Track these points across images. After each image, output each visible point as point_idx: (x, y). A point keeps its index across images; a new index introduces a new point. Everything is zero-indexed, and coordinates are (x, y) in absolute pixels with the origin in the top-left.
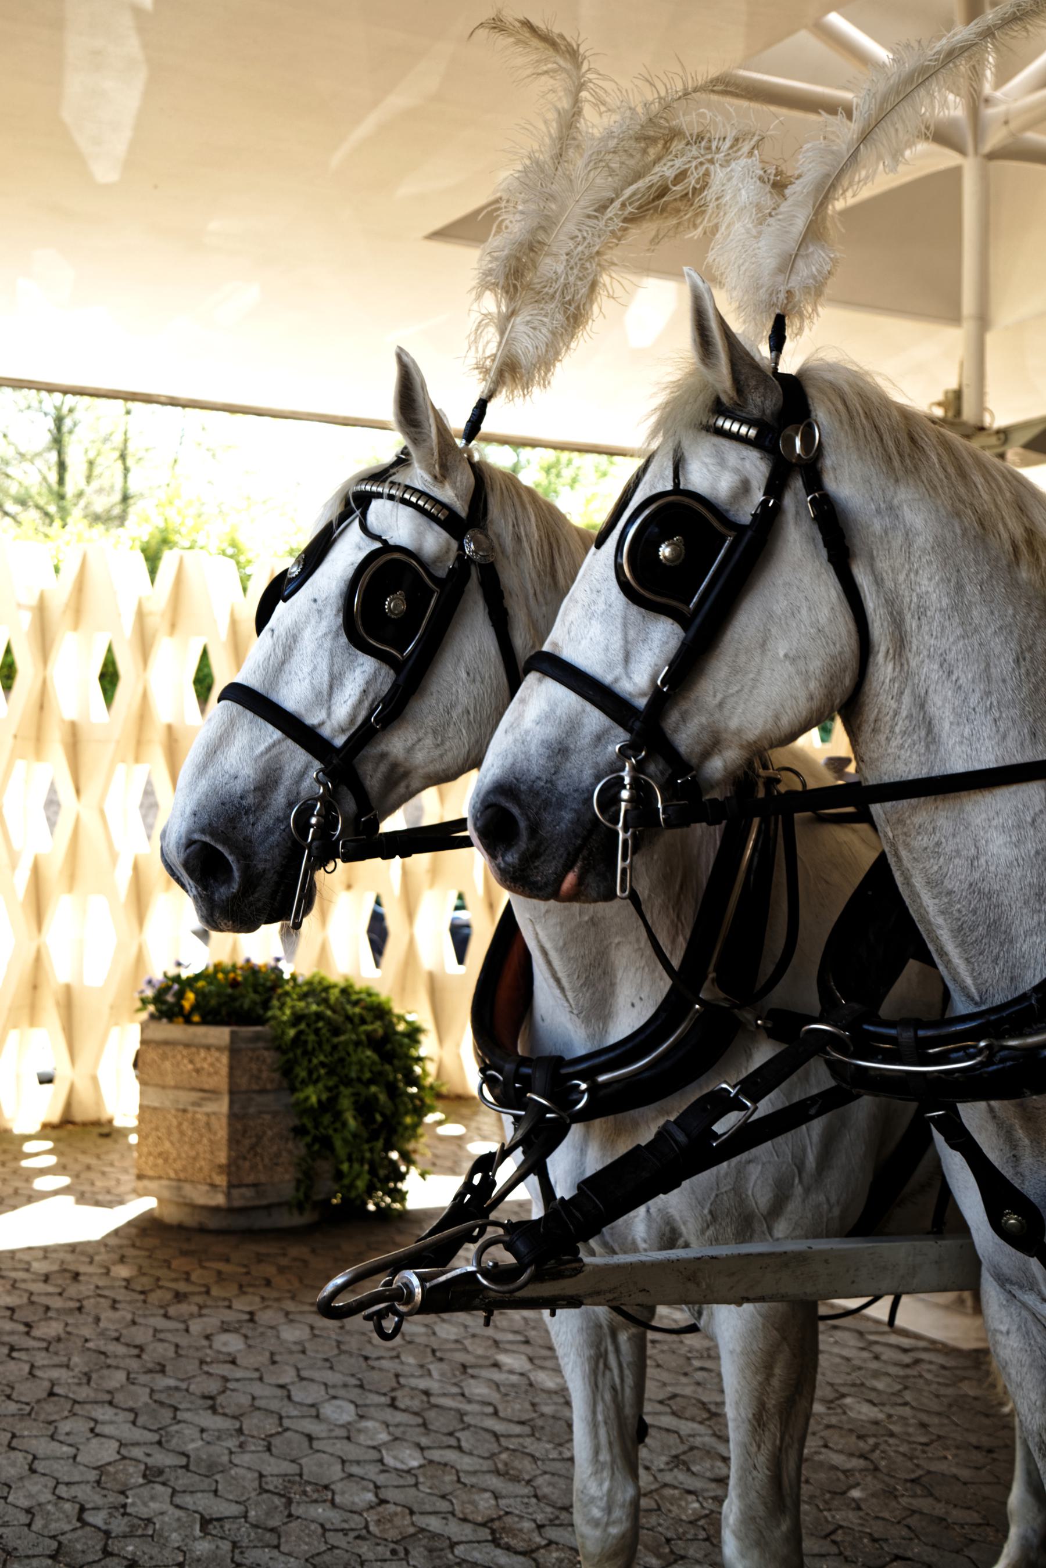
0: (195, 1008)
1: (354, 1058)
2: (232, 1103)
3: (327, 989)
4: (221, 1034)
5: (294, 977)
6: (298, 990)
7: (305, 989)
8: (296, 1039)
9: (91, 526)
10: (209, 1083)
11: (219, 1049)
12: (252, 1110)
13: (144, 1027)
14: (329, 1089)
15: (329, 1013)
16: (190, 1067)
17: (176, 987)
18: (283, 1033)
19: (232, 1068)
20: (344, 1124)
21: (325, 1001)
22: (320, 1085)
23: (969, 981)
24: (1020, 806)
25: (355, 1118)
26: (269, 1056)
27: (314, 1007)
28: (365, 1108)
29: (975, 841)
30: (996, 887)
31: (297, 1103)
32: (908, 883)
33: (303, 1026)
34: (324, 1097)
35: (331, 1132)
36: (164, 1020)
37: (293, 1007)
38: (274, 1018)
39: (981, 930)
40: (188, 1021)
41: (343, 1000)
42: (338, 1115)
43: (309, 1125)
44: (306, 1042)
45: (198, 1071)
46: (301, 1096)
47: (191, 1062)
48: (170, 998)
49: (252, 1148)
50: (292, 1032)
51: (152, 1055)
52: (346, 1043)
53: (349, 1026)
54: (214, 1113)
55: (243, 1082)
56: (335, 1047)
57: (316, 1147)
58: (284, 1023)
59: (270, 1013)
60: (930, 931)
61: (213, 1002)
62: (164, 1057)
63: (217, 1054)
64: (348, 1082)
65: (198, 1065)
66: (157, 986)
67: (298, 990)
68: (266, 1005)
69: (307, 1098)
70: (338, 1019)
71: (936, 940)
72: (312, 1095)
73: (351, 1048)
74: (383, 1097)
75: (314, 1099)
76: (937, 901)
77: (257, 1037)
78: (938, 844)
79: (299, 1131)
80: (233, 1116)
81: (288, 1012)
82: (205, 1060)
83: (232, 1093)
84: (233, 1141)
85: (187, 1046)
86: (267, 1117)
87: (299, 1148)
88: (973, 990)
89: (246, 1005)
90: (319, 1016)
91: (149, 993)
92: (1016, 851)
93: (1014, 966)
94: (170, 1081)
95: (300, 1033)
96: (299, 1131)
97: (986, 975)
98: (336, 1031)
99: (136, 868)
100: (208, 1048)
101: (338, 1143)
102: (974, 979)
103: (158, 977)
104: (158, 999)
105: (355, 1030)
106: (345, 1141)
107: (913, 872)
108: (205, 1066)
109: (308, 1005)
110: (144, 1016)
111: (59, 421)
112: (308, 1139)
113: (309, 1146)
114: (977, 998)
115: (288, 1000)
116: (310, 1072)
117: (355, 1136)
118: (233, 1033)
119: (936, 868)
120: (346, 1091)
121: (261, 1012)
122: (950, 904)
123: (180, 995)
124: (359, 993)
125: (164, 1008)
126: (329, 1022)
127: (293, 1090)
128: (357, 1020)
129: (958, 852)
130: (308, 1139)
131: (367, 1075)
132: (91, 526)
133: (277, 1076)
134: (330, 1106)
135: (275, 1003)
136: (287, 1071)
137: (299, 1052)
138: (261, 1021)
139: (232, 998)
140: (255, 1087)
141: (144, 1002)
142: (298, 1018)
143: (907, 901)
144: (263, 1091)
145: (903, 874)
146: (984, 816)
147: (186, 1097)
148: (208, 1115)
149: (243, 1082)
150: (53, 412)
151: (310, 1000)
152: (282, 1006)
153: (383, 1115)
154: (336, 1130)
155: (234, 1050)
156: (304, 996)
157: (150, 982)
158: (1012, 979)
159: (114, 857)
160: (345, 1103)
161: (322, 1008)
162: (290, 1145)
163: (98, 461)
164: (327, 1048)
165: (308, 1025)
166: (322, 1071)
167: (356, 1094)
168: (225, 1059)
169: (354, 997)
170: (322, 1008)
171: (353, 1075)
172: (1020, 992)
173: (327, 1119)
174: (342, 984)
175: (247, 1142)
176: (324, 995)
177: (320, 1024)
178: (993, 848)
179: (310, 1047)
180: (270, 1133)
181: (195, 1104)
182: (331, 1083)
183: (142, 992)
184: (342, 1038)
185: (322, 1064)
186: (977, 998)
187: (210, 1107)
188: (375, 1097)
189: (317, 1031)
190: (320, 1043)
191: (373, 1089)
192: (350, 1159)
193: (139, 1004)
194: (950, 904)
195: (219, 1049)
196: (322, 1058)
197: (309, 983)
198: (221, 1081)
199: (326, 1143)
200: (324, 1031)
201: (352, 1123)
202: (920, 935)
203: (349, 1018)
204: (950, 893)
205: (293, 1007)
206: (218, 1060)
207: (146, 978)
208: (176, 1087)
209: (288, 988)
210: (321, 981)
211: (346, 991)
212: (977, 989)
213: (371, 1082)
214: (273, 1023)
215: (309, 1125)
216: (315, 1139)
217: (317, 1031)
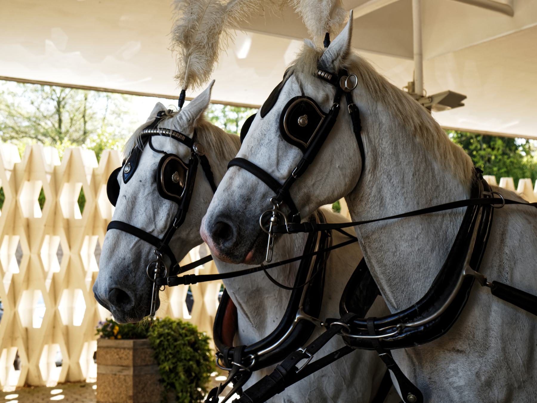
0: (119, 332)
1: (183, 351)
2: (134, 371)
3: (172, 323)
4: (129, 343)
5: (158, 319)
6: (160, 324)
7: (163, 323)
8: (160, 344)
9: (72, 144)
10: (125, 363)
11: (129, 349)
12: (142, 373)
13: (98, 341)
14: (173, 363)
15: (172, 333)
16: (117, 357)
17: (111, 324)
18: (154, 342)
19: (134, 356)
20: (180, 377)
21: (171, 328)
22: (170, 362)
23: (393, 301)
24: (413, 232)
25: (184, 375)
26: (149, 351)
27: (167, 331)
28: (188, 371)
29: (396, 245)
30: (403, 263)
31: (160, 370)
32: (370, 262)
33: (162, 338)
34: (172, 366)
35: (174, 381)
36: (107, 338)
37: (158, 331)
38: (151, 335)
39: (397, 280)
40: (116, 338)
41: (178, 327)
42: (177, 374)
43: (166, 378)
44: (163, 345)
45: (120, 358)
46: (162, 366)
47: (118, 354)
48: (109, 329)
49: (143, 388)
50: (158, 341)
51: (102, 352)
52: (180, 345)
53: (181, 338)
54: (127, 375)
55: (139, 362)
56: (175, 347)
57: (169, 387)
58: (155, 337)
59: (149, 334)
60: (378, 281)
61: (126, 330)
62: (107, 353)
63: (127, 351)
64: (180, 360)
65: (121, 356)
66: (104, 324)
67: (160, 324)
68: (147, 330)
69: (165, 368)
70: (176, 335)
71: (380, 284)
72: (167, 366)
73: (182, 347)
74: (195, 366)
75: (167, 368)
76: (380, 269)
77: (144, 344)
78: (381, 246)
79: (162, 381)
80: (135, 376)
81: (156, 333)
82: (123, 354)
83: (134, 367)
84: (135, 386)
85: (116, 348)
86: (149, 376)
87: (161, 388)
88: (394, 304)
89: (139, 330)
90: (169, 334)
91: (100, 327)
92: (411, 249)
93: (410, 294)
94: (109, 363)
95: (161, 341)
96: (162, 381)
97: (399, 298)
98: (176, 340)
99: (93, 278)
100: (124, 348)
101: (177, 385)
102: (395, 299)
103: (103, 320)
104: (104, 329)
105: (183, 339)
106: (180, 384)
107: (371, 257)
108: (123, 356)
109: (164, 330)
110: (98, 337)
111: (59, 103)
112: (165, 384)
113: (165, 387)
114: (396, 307)
115: (156, 329)
116: (166, 357)
117: (184, 382)
118: (134, 342)
119: (380, 256)
120: (180, 364)
121: (145, 333)
122: (385, 270)
123: (113, 328)
124: (184, 324)
125: (107, 333)
126: (173, 336)
127: (159, 364)
128: (184, 335)
129: (389, 249)
130: (165, 384)
131: (188, 357)
132: (72, 144)
133: (152, 359)
134: (173, 370)
135: (151, 329)
136: (156, 357)
137: (161, 349)
138: (145, 337)
139: (134, 328)
140: (143, 364)
141: (98, 331)
142: (160, 335)
143: (370, 269)
144: (147, 365)
145: (367, 258)
146: (399, 236)
147: (116, 369)
148: (125, 376)
149: (139, 362)
150: (57, 99)
151: (165, 328)
152: (154, 331)
153: (195, 373)
154: (176, 380)
155: (135, 349)
156: (162, 326)
157: (100, 323)
158: (409, 299)
159: (85, 273)
160: (180, 369)
161: (170, 331)
162: (158, 387)
163: (75, 118)
164: (172, 347)
165: (164, 338)
166: (170, 356)
167: (184, 365)
168: (131, 353)
169: (182, 326)
170: (170, 331)
171: (183, 357)
172: (412, 304)
173: (172, 375)
174: (177, 321)
175: (141, 386)
176: (170, 326)
177: (169, 337)
178: (402, 248)
179: (165, 347)
180: (150, 382)
181: (119, 372)
182: (174, 361)
183: (97, 327)
184: (178, 343)
185: (171, 354)
186: (396, 307)
187: (126, 373)
188: (192, 366)
189: (168, 340)
190: (169, 345)
191: (191, 363)
192: (182, 391)
193: (96, 332)
194: (385, 270)
195: (129, 349)
196: (170, 351)
197: (164, 321)
198: (129, 362)
199: (173, 385)
200: (171, 340)
201: (183, 377)
202: (375, 283)
203: (181, 335)
204: (385, 265)
205: (158, 331)
206: (128, 353)
207: (99, 321)
208: (112, 365)
209: (156, 323)
210: (169, 320)
211: (179, 324)
212: (396, 303)
213: (190, 360)
214: (150, 337)
215: (166, 378)
216: (168, 384)
217: (168, 340)
